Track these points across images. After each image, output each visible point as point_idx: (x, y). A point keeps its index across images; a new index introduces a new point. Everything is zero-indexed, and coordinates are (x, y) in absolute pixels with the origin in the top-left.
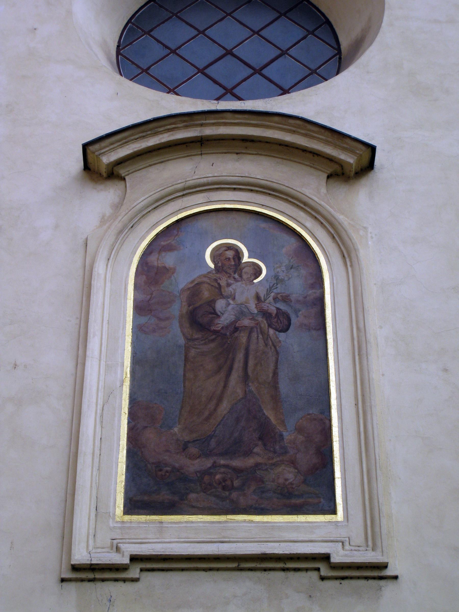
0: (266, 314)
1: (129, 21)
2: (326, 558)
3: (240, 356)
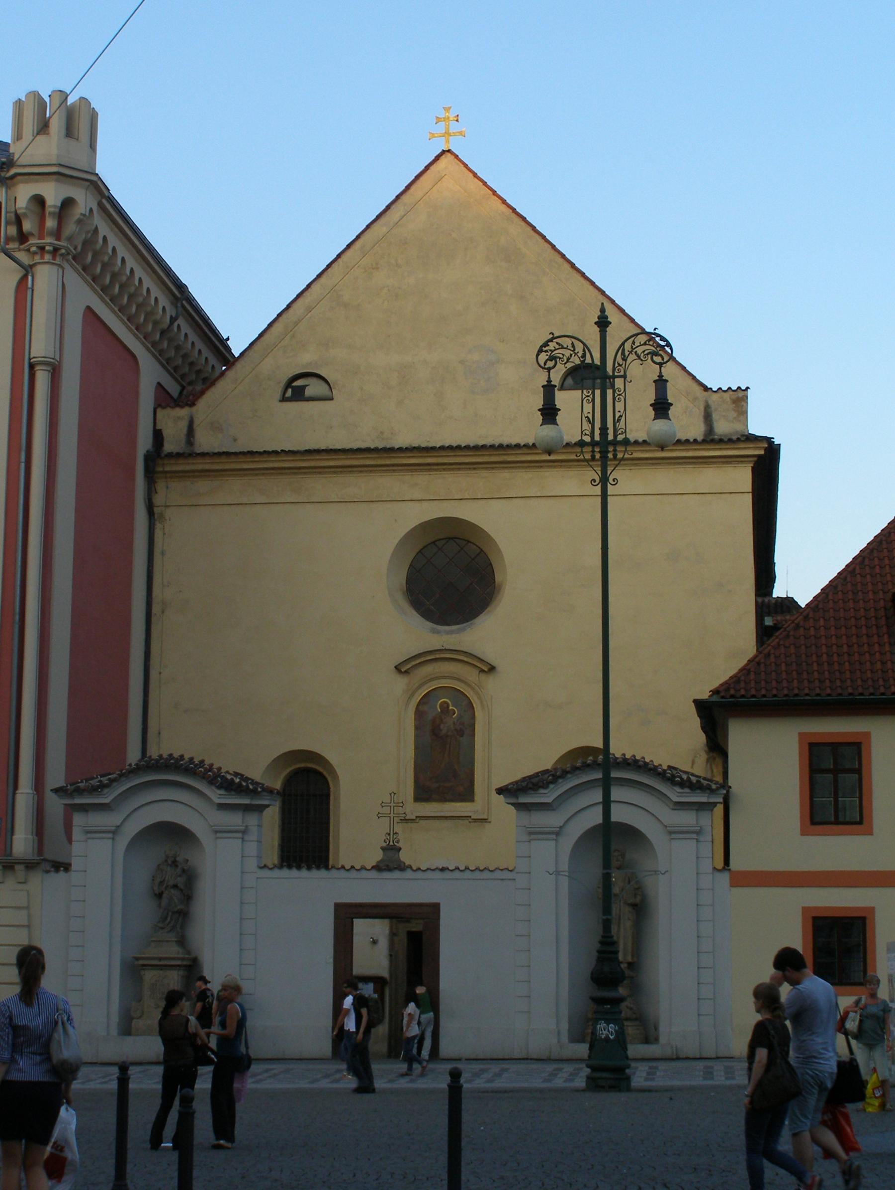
0: (456, 730)
1: (411, 565)
2: (470, 817)
3: (448, 746)
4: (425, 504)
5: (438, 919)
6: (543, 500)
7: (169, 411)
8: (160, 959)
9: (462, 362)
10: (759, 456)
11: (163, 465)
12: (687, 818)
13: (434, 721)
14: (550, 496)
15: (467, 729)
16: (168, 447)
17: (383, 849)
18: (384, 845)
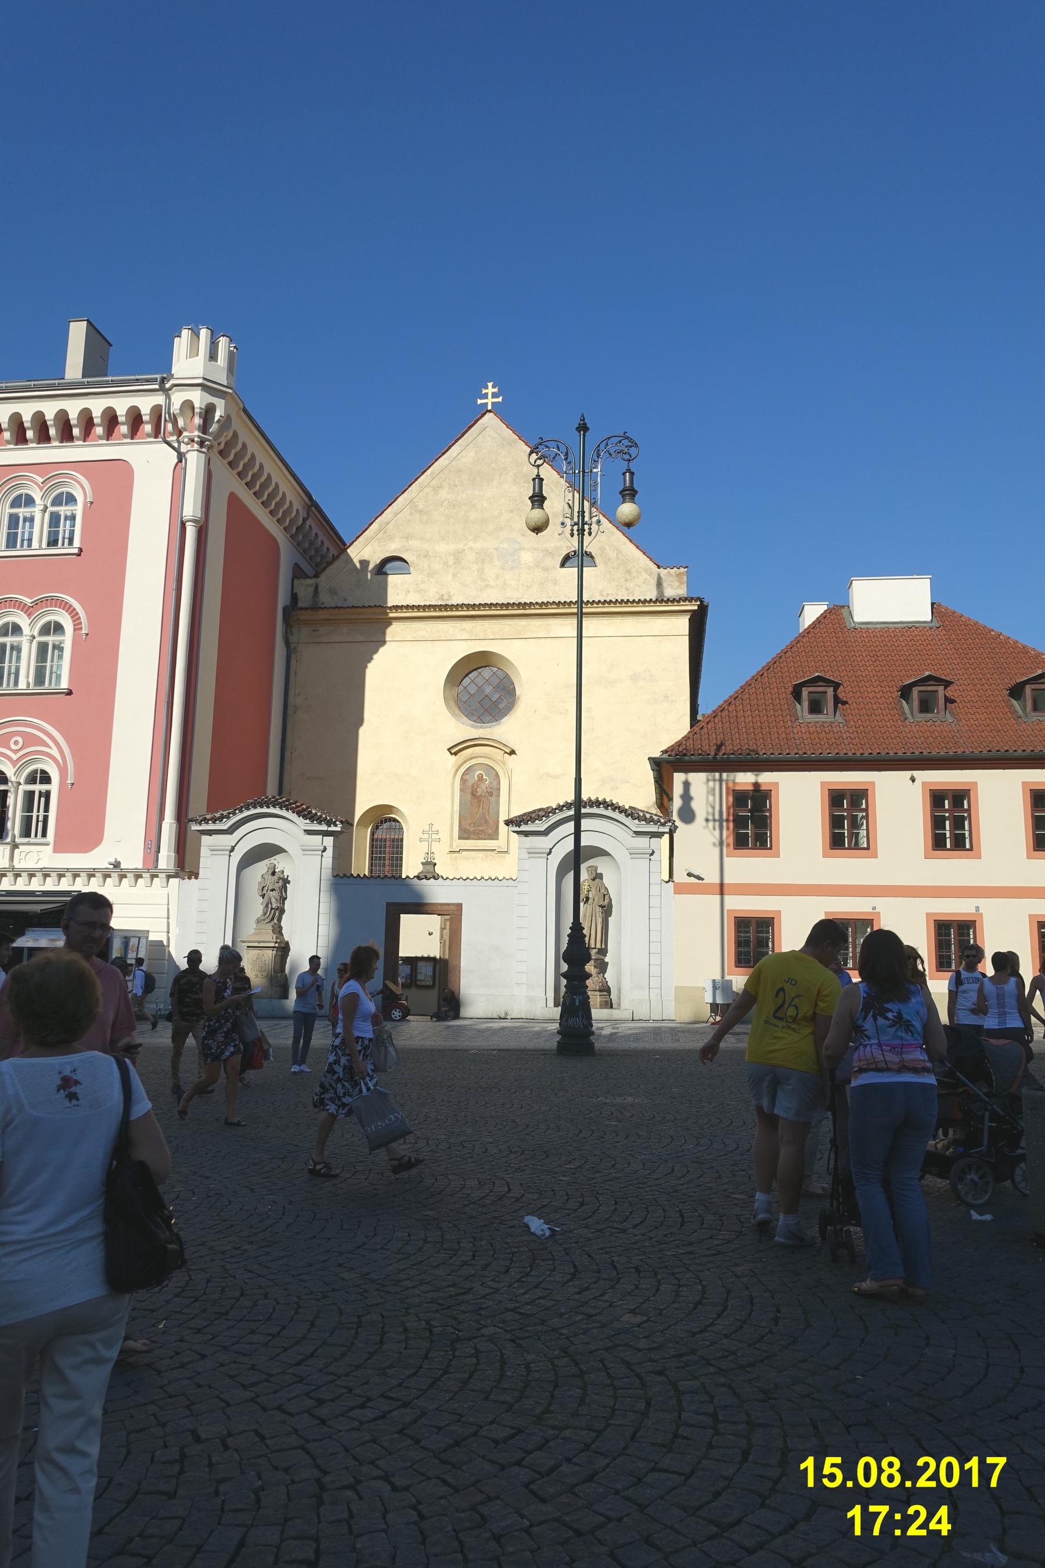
0: (487, 792)
8: (259, 942)
9: (496, 549)
10: (693, 611)
12: (643, 842)
13: (473, 786)
15: (494, 792)
16: (300, 604)
17: (423, 864)
18: (424, 861)
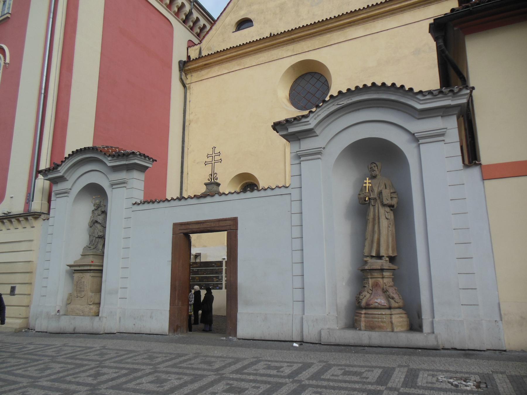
4: (292, 57)
5: (237, 230)
6: (347, 42)
7: (192, 48)
11: (188, 66)
14: (350, 40)
17: (206, 184)
